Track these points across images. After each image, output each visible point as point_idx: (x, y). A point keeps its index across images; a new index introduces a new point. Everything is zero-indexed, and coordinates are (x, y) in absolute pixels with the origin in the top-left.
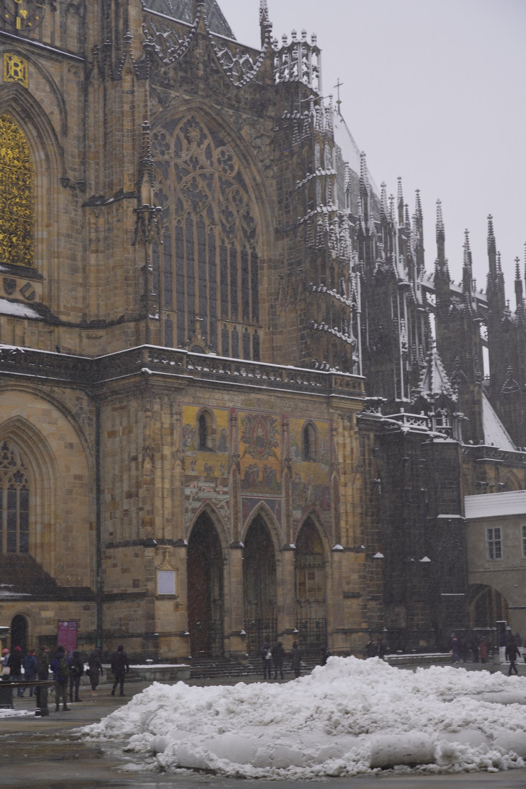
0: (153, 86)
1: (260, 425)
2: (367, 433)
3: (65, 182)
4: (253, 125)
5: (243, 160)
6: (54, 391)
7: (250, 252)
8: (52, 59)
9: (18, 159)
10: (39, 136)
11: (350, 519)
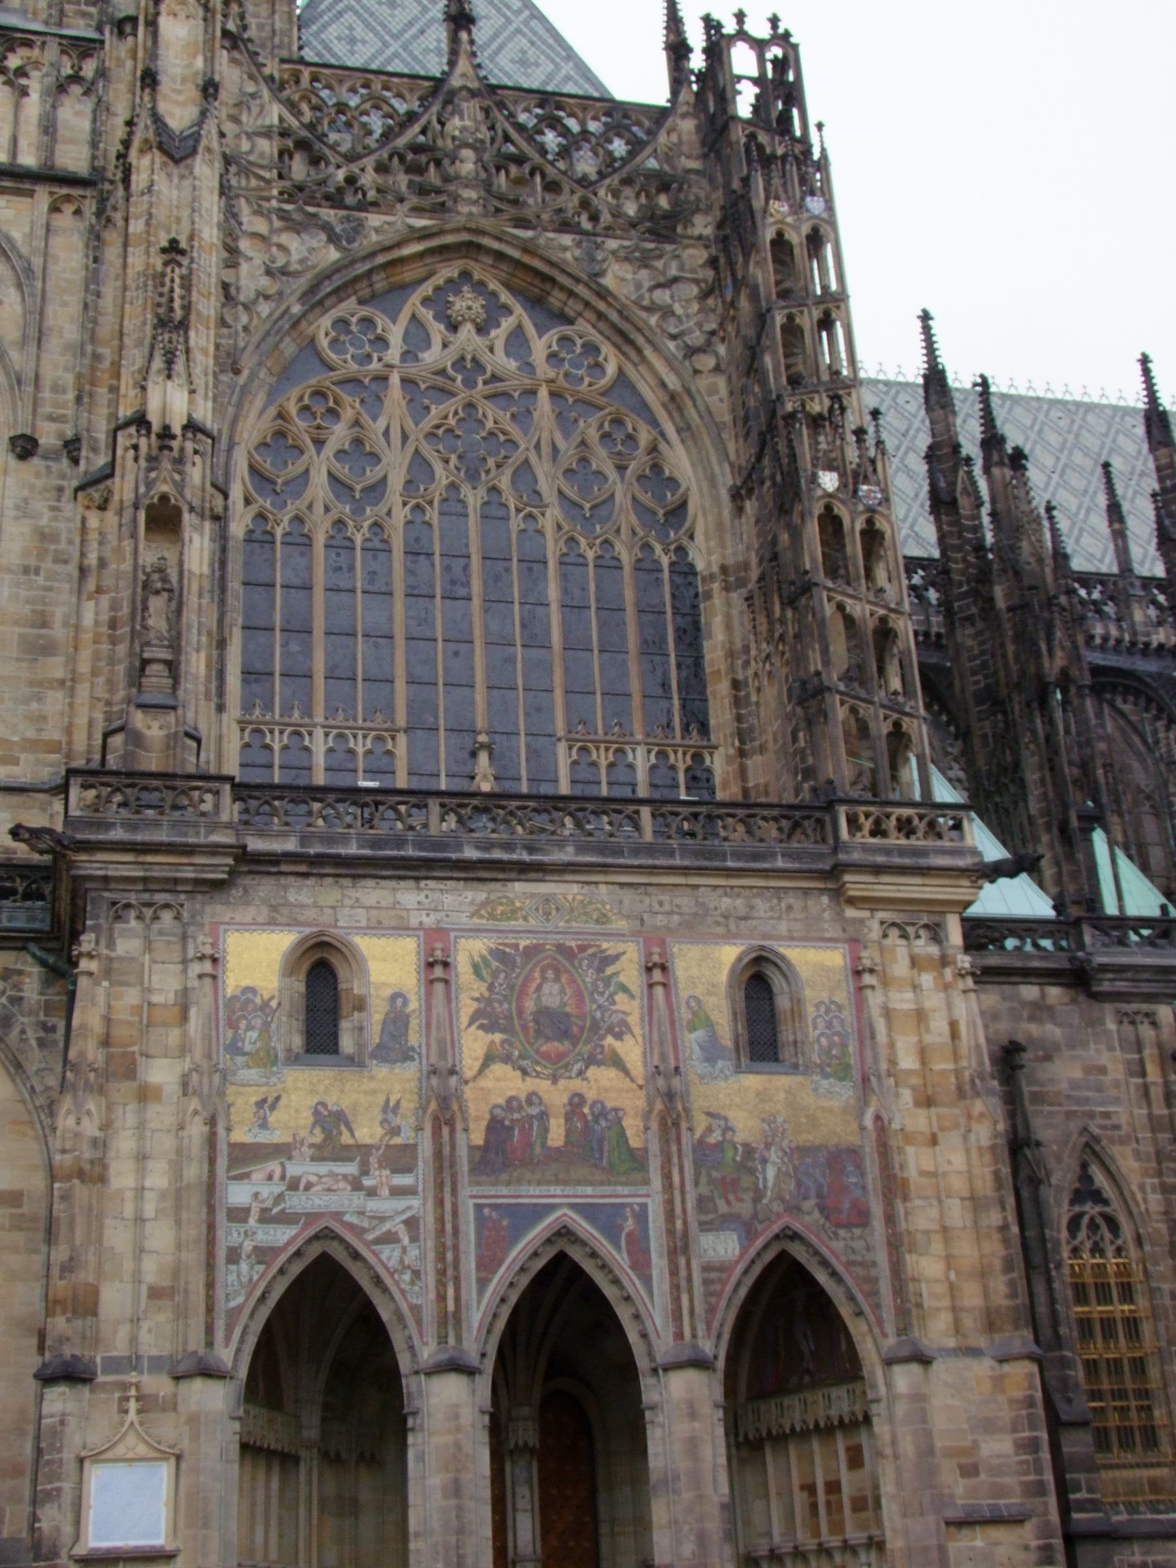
0: (311, 210)
1: (550, 974)
2: (1145, 1007)
4: (644, 261)
5: (627, 349)
7: (665, 561)
11: (967, 1251)
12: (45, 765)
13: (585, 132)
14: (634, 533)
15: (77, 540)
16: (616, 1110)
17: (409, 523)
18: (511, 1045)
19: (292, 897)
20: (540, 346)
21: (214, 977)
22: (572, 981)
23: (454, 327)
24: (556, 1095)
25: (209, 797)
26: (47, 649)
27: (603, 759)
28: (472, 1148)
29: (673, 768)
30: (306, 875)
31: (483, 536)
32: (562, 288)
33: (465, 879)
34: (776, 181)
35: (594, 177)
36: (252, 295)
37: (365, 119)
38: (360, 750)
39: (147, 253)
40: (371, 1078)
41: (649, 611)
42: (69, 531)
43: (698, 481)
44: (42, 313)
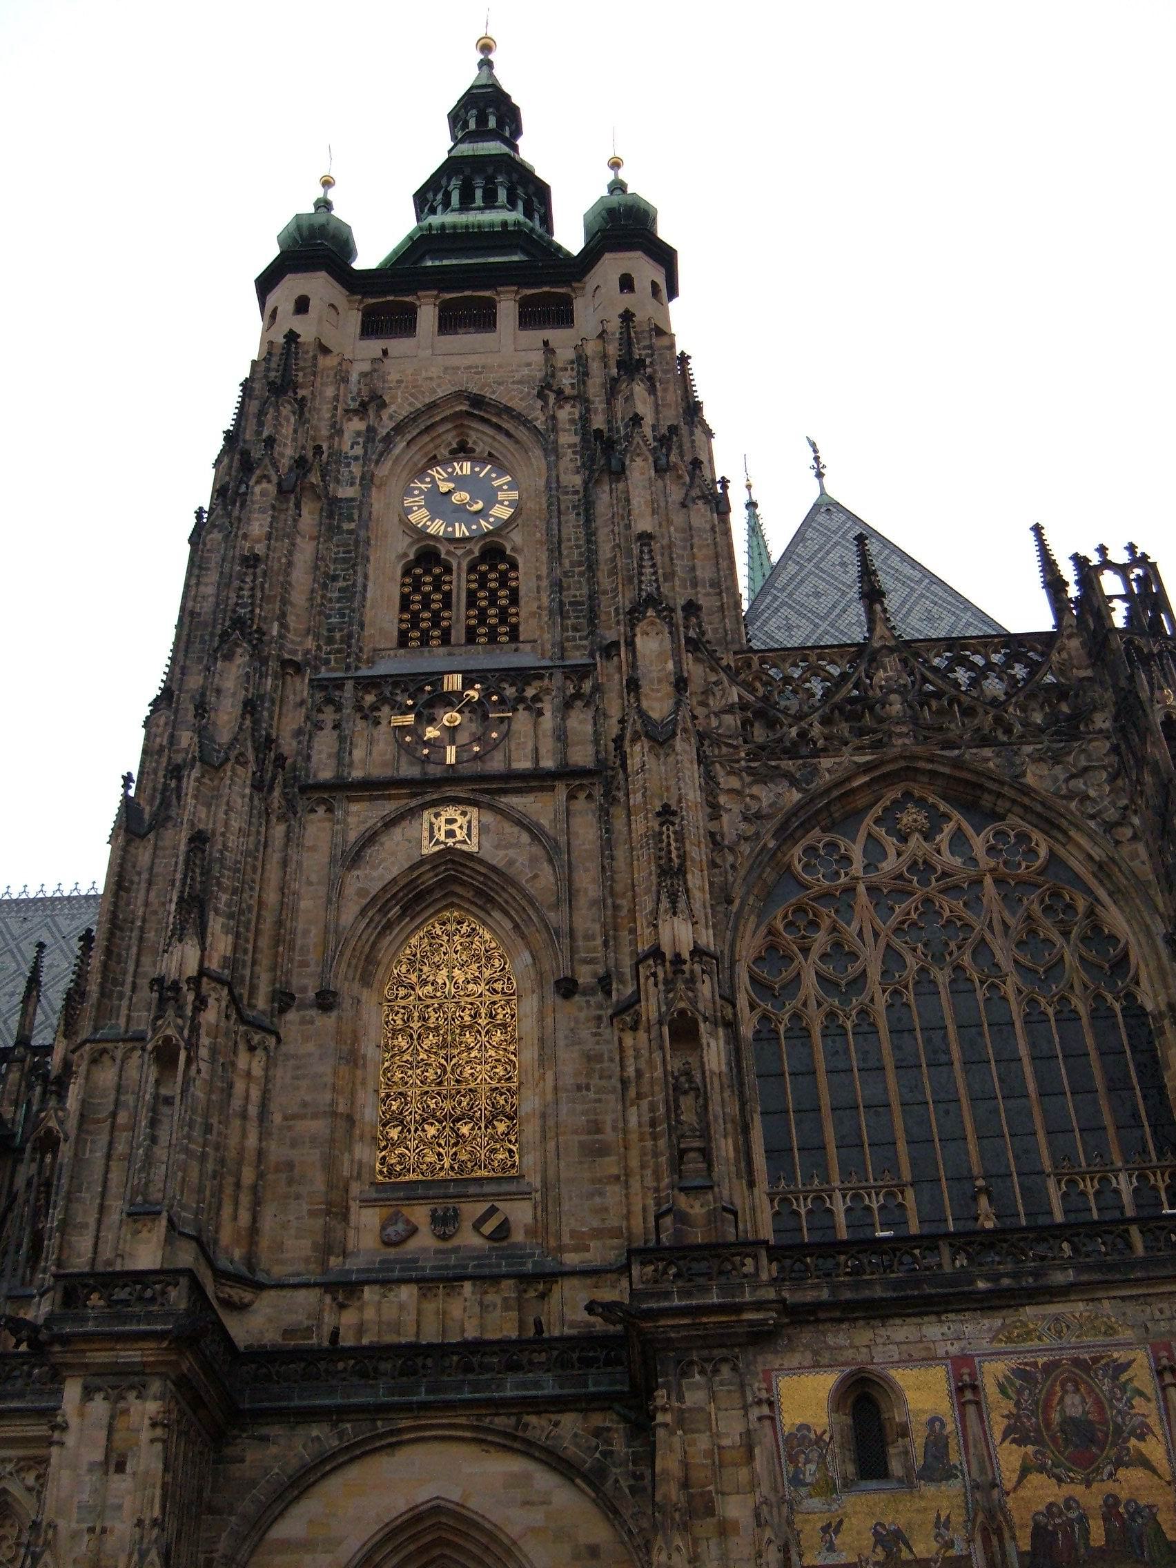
1: (1070, 1386)
3: (567, 988)
4: (1057, 759)
5: (1055, 833)
6: (526, 1425)
7: (1117, 1007)
8: (531, 790)
9: (476, 981)
10: (516, 926)
12: (613, 1248)
13: (990, 666)
14: (1086, 987)
15: (617, 1058)
16: (1150, 1507)
17: (889, 1007)
18: (1043, 1455)
19: (831, 1340)
20: (979, 844)
21: (772, 1419)
22: (1091, 1391)
23: (904, 839)
24: (1092, 1498)
25: (748, 1261)
26: (602, 1151)
27: (1090, 1188)
28: (1021, 1554)
29: (1155, 1188)
30: (840, 1321)
31: (954, 1006)
32: (990, 792)
33: (981, 1309)
34: (1157, 674)
35: (1003, 698)
36: (735, 837)
37: (807, 685)
38: (875, 1206)
39: (646, 818)
40: (921, 1497)
41: (1109, 1052)
42: (610, 1051)
43: (1135, 934)
44: (570, 880)
